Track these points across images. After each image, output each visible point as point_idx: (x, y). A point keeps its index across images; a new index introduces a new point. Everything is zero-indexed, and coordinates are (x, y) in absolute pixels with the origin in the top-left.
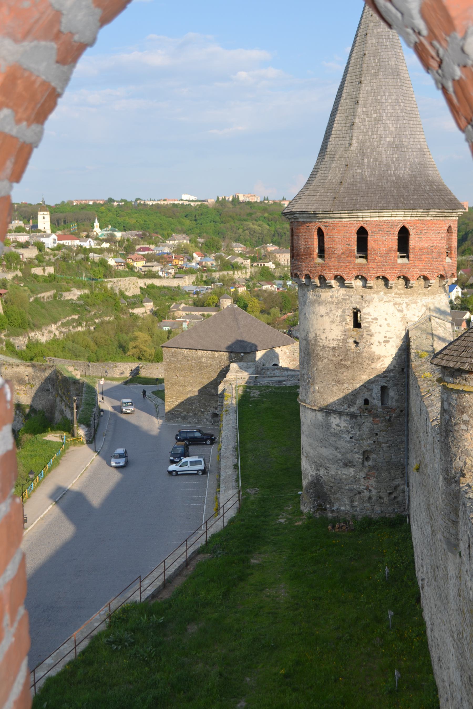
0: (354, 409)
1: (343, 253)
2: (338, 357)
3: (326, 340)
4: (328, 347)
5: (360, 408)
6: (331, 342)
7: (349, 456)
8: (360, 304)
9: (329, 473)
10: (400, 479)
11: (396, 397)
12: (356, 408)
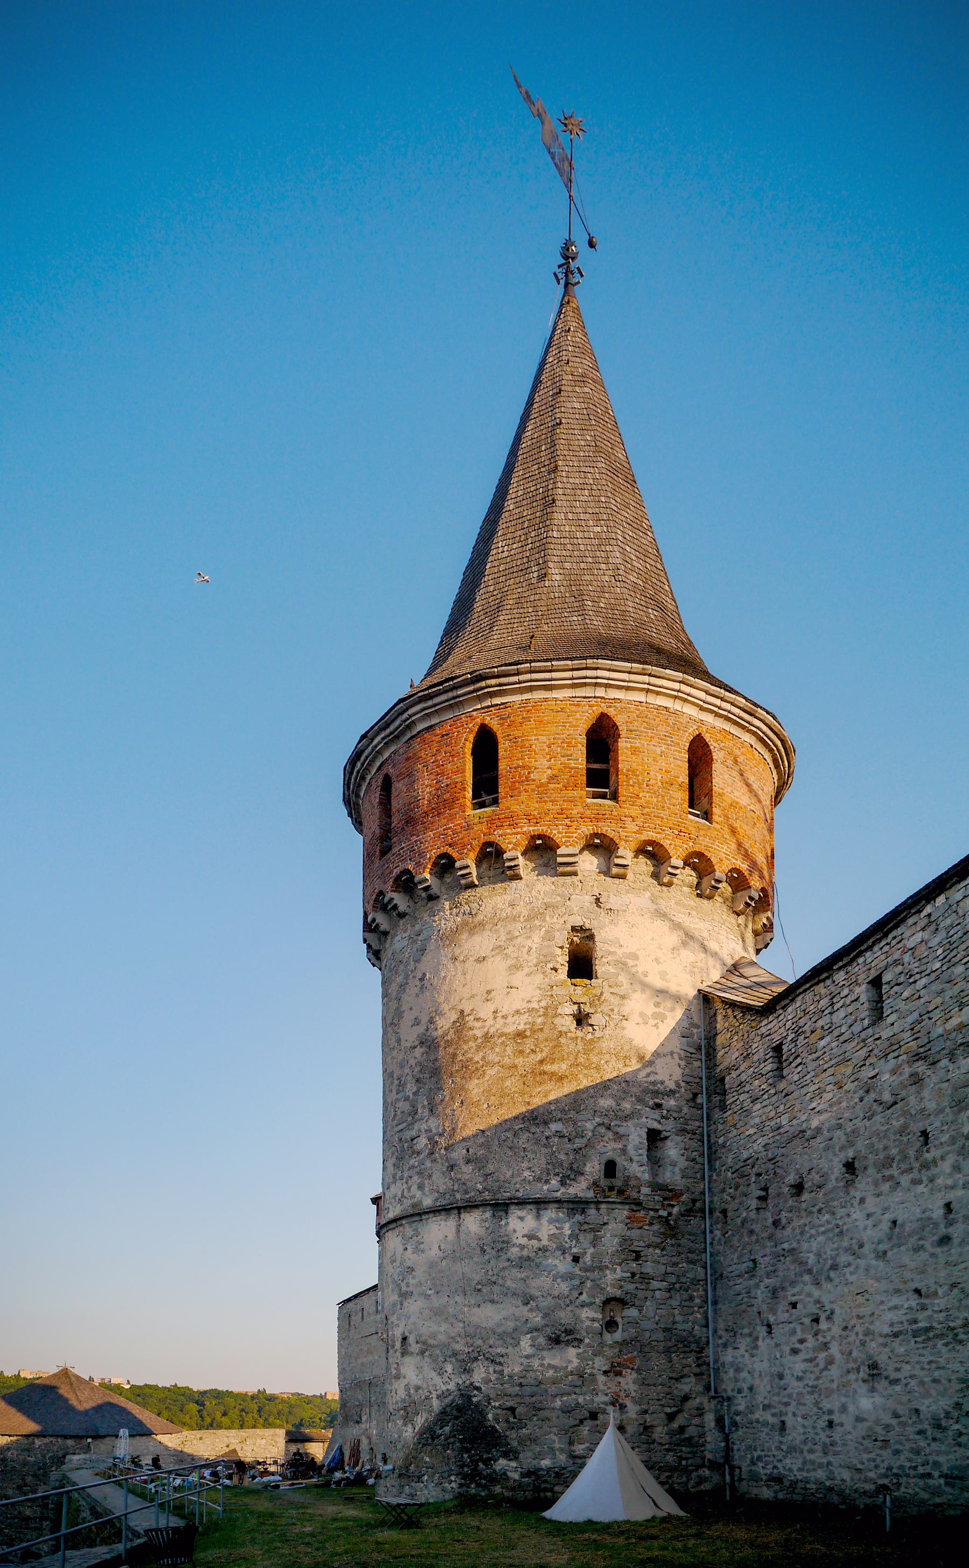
0: (579, 1189)
1: (552, 778)
2: (533, 1056)
3: (495, 1018)
4: (502, 1035)
5: (595, 1184)
6: (510, 1019)
7: (564, 1317)
8: (592, 916)
9: (501, 1373)
10: (693, 1379)
11: (682, 1163)
12: (584, 1185)
